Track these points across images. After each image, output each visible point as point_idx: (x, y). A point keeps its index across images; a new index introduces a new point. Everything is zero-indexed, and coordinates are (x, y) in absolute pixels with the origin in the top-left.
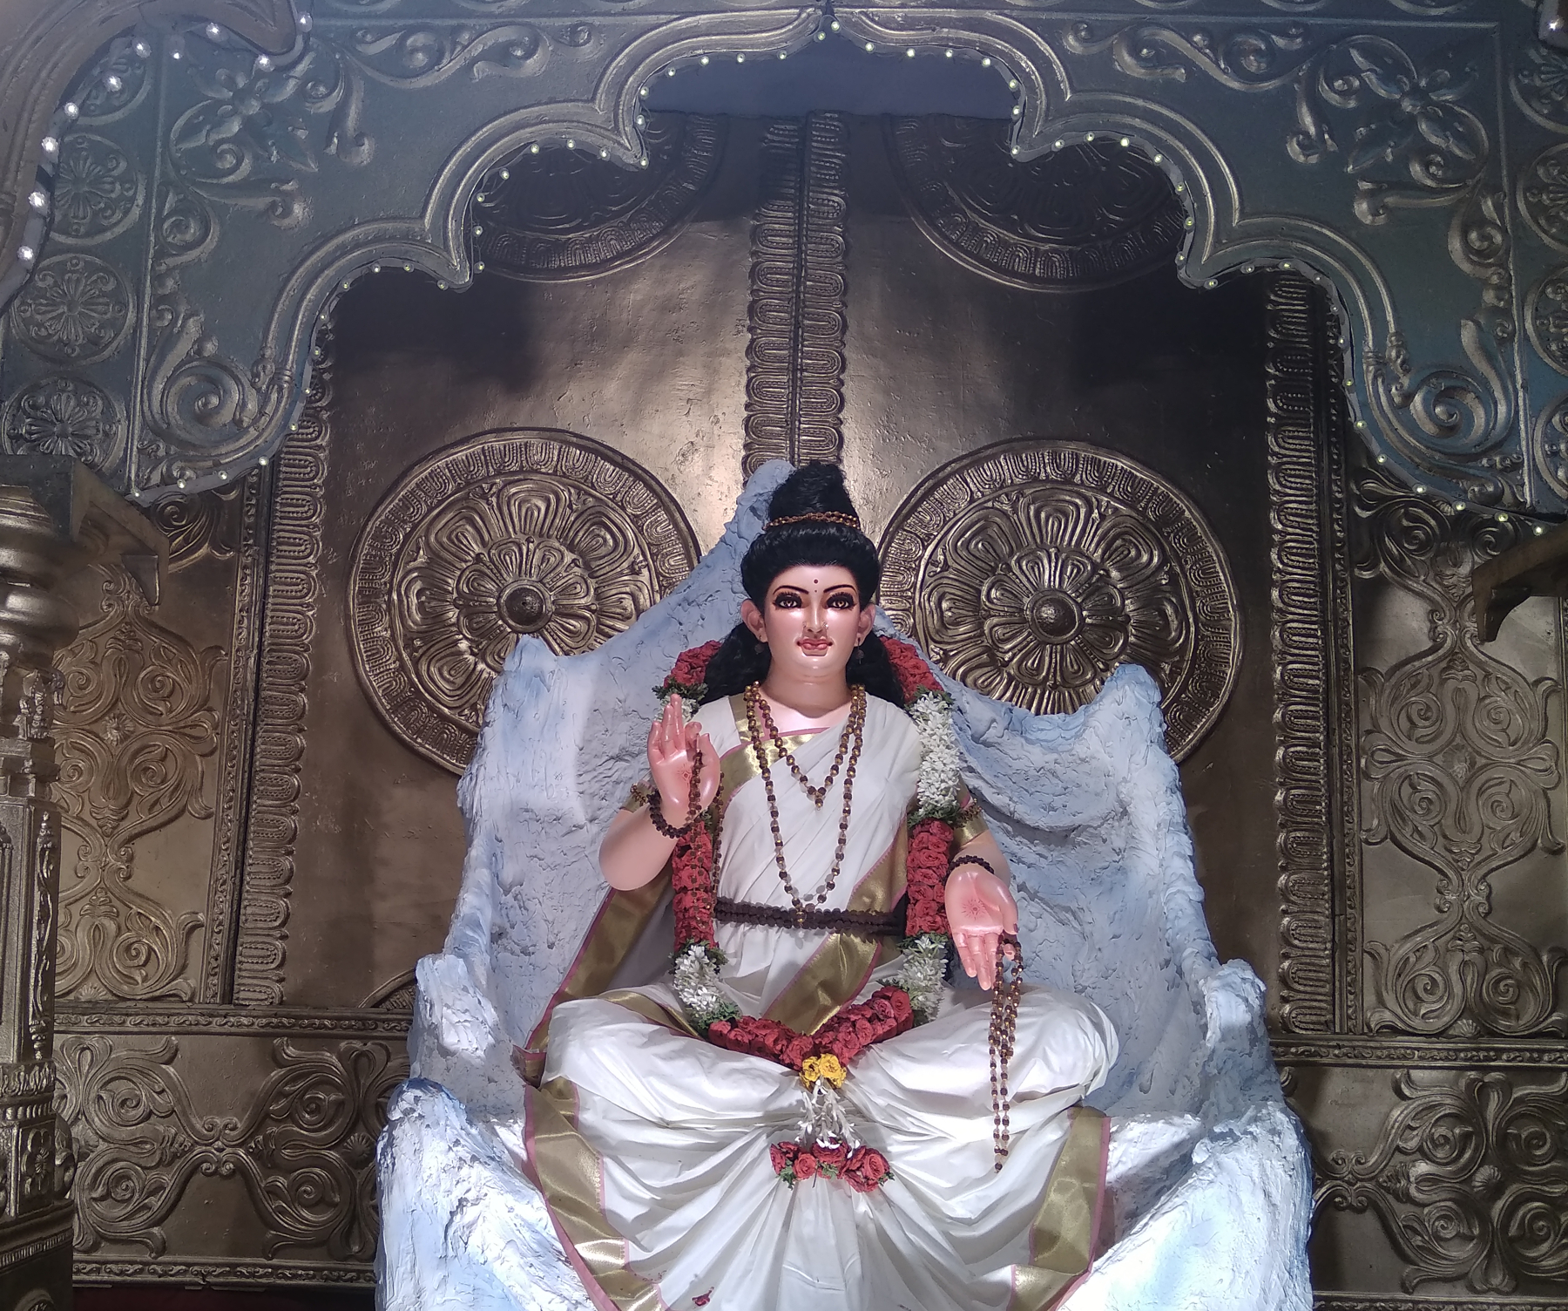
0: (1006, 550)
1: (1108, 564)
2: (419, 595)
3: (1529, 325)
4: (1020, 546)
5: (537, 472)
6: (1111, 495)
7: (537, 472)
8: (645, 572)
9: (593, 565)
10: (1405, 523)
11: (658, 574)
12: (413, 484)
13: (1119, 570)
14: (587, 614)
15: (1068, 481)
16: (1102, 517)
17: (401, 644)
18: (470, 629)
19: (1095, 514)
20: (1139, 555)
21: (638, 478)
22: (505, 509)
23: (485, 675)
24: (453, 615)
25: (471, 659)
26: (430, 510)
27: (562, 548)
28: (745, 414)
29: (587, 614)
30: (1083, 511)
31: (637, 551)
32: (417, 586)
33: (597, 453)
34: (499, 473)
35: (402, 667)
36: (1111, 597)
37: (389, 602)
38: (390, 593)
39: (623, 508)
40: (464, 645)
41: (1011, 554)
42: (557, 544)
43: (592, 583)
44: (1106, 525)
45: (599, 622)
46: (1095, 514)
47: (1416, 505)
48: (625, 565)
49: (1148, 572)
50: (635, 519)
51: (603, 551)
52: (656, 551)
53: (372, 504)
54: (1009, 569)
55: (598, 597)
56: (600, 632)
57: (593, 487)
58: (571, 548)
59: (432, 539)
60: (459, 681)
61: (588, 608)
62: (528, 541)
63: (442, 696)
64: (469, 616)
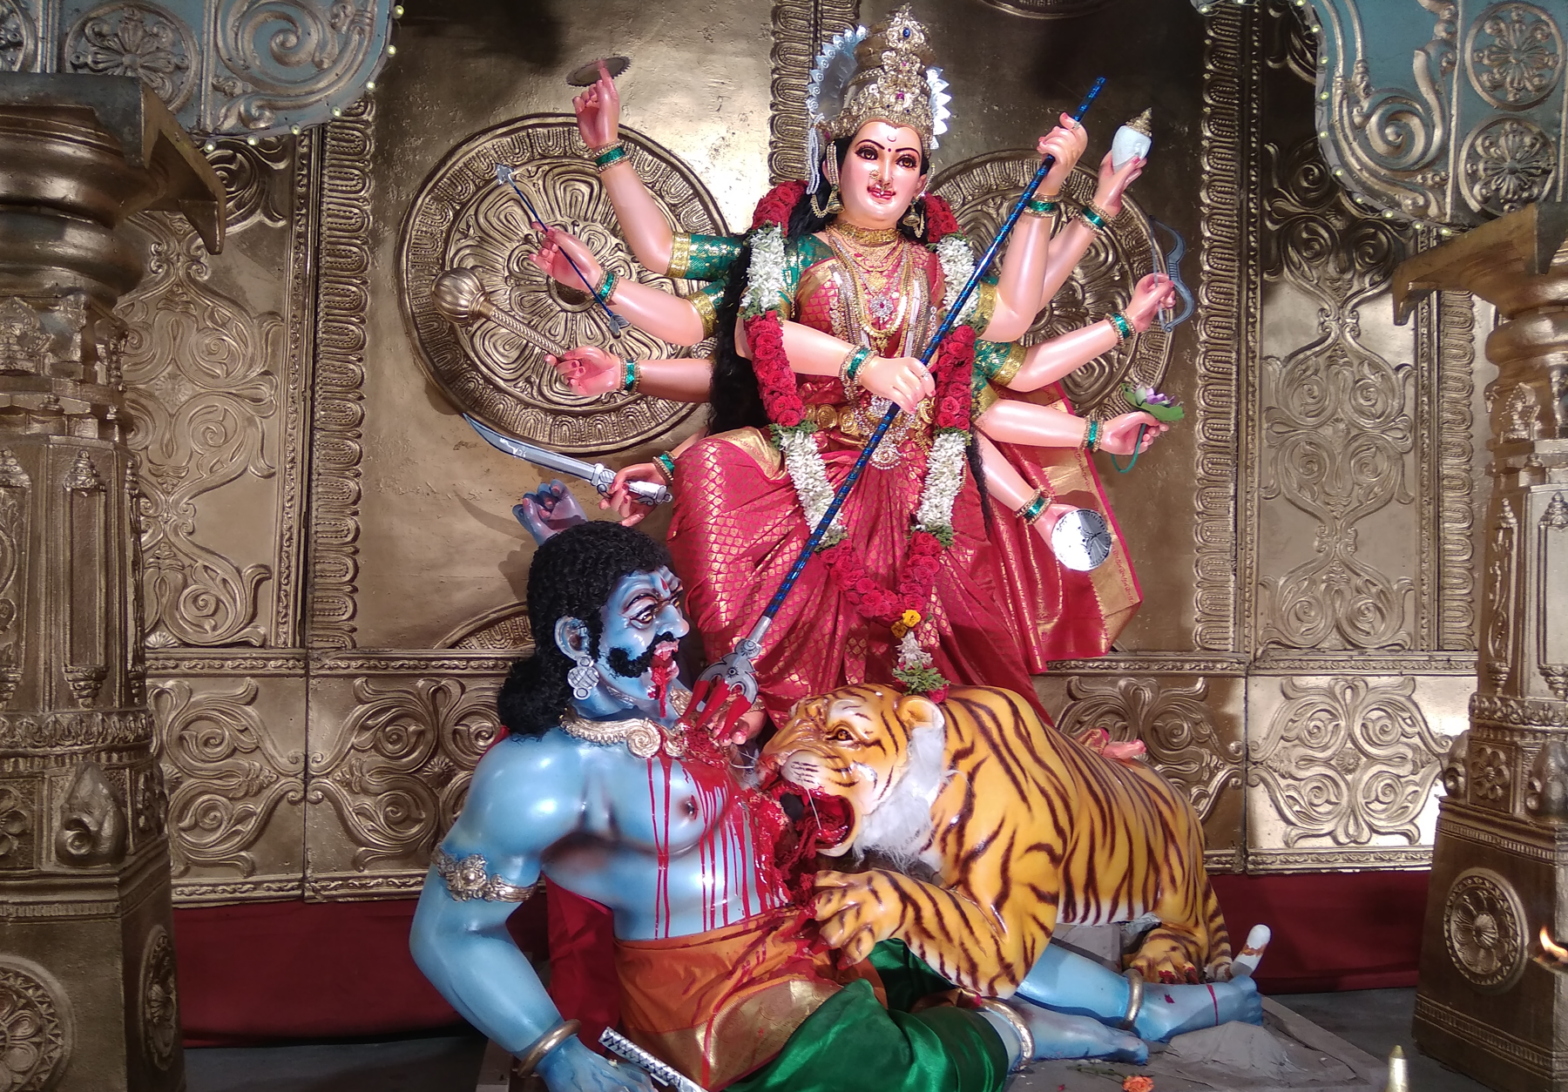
5: (580, 157)
7: (580, 157)
10: (1305, 235)
12: (460, 164)
19: (1064, 219)
20: (1098, 254)
22: (551, 192)
26: (479, 189)
27: (607, 232)
28: (771, 113)
33: (637, 143)
36: (1075, 291)
42: (600, 228)
46: (1064, 219)
47: (1314, 220)
49: (1103, 269)
53: (420, 181)
58: (614, 232)
59: (482, 220)
60: (515, 354)
62: (574, 224)
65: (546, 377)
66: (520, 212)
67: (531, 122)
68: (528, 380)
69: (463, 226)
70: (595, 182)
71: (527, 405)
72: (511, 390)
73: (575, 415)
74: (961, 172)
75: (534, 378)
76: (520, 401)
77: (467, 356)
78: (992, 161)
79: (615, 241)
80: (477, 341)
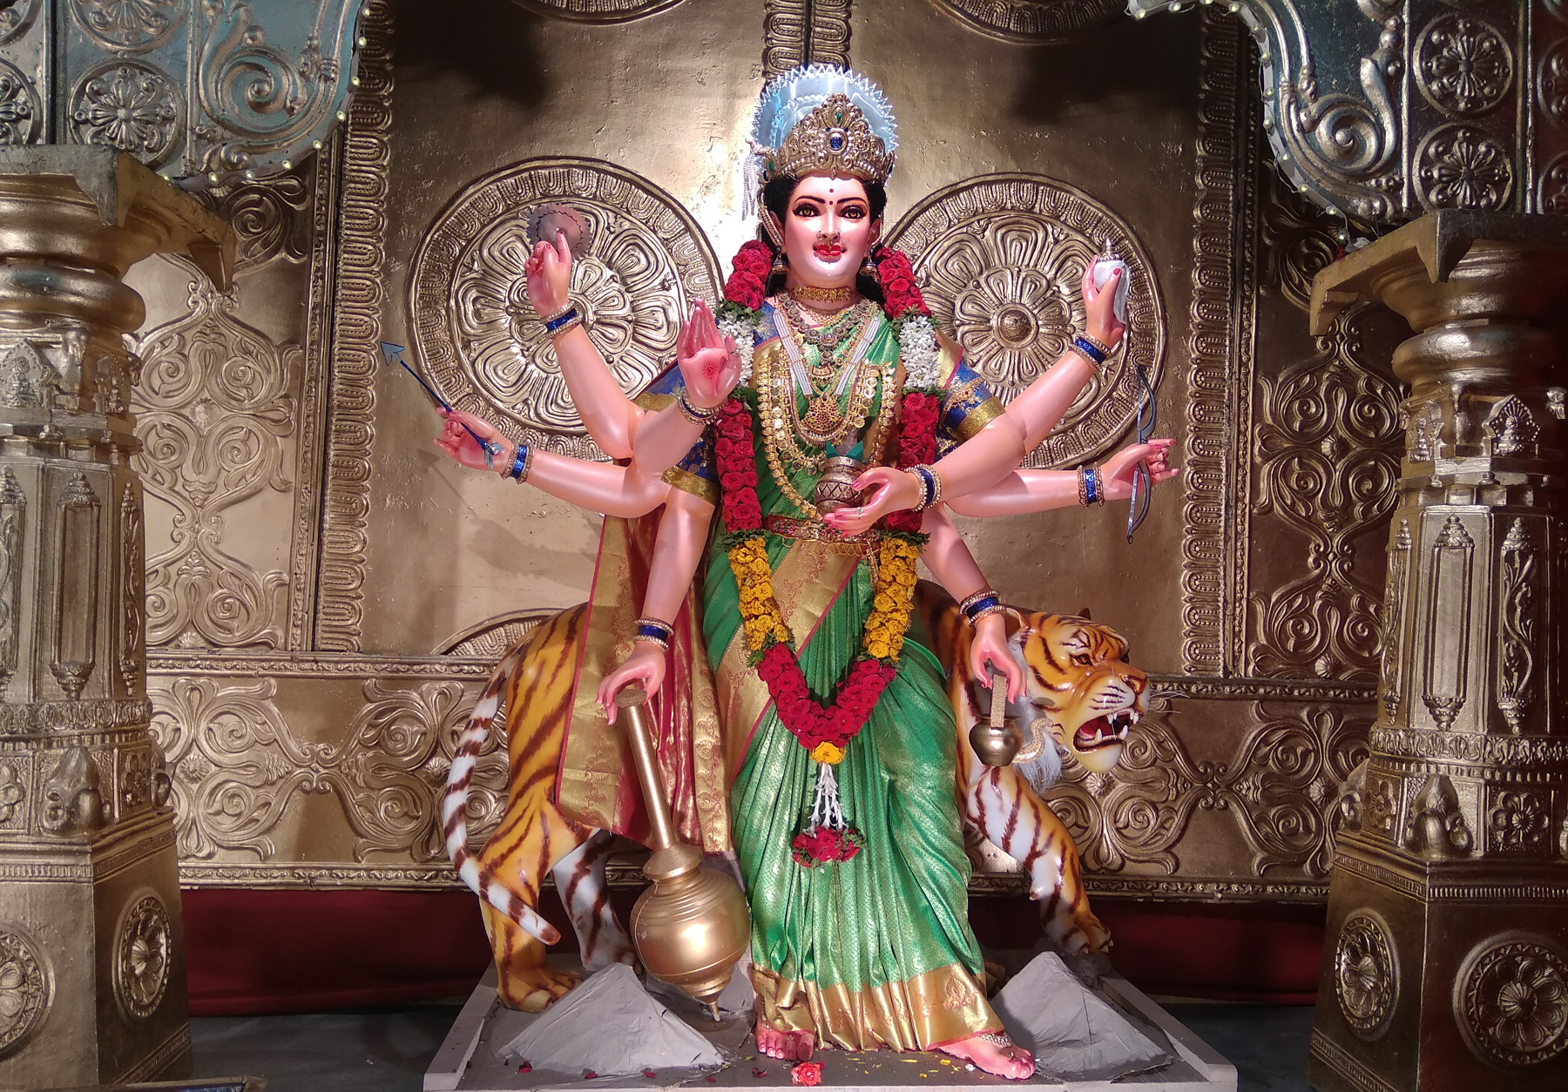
0: (976, 269)
1: (1059, 282)
2: (475, 301)
3: (1416, 66)
4: (988, 266)
5: (579, 196)
6: (1064, 222)
7: (579, 196)
8: (674, 288)
9: (629, 281)
11: (685, 291)
13: (1069, 286)
14: (624, 324)
15: (1030, 210)
16: (1057, 241)
17: (459, 345)
18: (521, 334)
19: (1051, 239)
21: (668, 205)
23: (535, 375)
24: (505, 320)
25: (523, 361)
27: (603, 265)
29: (624, 324)
30: (1041, 235)
31: (667, 269)
32: (473, 294)
34: (544, 196)
35: (461, 366)
37: (448, 309)
38: (448, 300)
39: (655, 232)
40: (516, 349)
41: (981, 273)
42: (597, 262)
43: (628, 297)
44: (1058, 249)
45: (635, 331)
46: (1051, 239)
48: (657, 282)
50: (665, 242)
51: (636, 269)
52: (683, 270)
53: (429, 220)
54: (979, 286)
55: (633, 310)
56: (635, 339)
57: (628, 212)
58: (610, 265)
59: (485, 253)
60: (513, 379)
61: (625, 318)
63: (496, 392)
64: (520, 323)
65: (542, 400)
66: (520, 246)
67: (537, 163)
68: (525, 402)
69: (467, 260)
70: (592, 219)
71: (524, 426)
72: (510, 411)
73: (570, 435)
74: (947, 196)
75: (532, 402)
76: (518, 422)
77: (471, 382)
78: (979, 184)
79: (608, 273)
80: (479, 367)
